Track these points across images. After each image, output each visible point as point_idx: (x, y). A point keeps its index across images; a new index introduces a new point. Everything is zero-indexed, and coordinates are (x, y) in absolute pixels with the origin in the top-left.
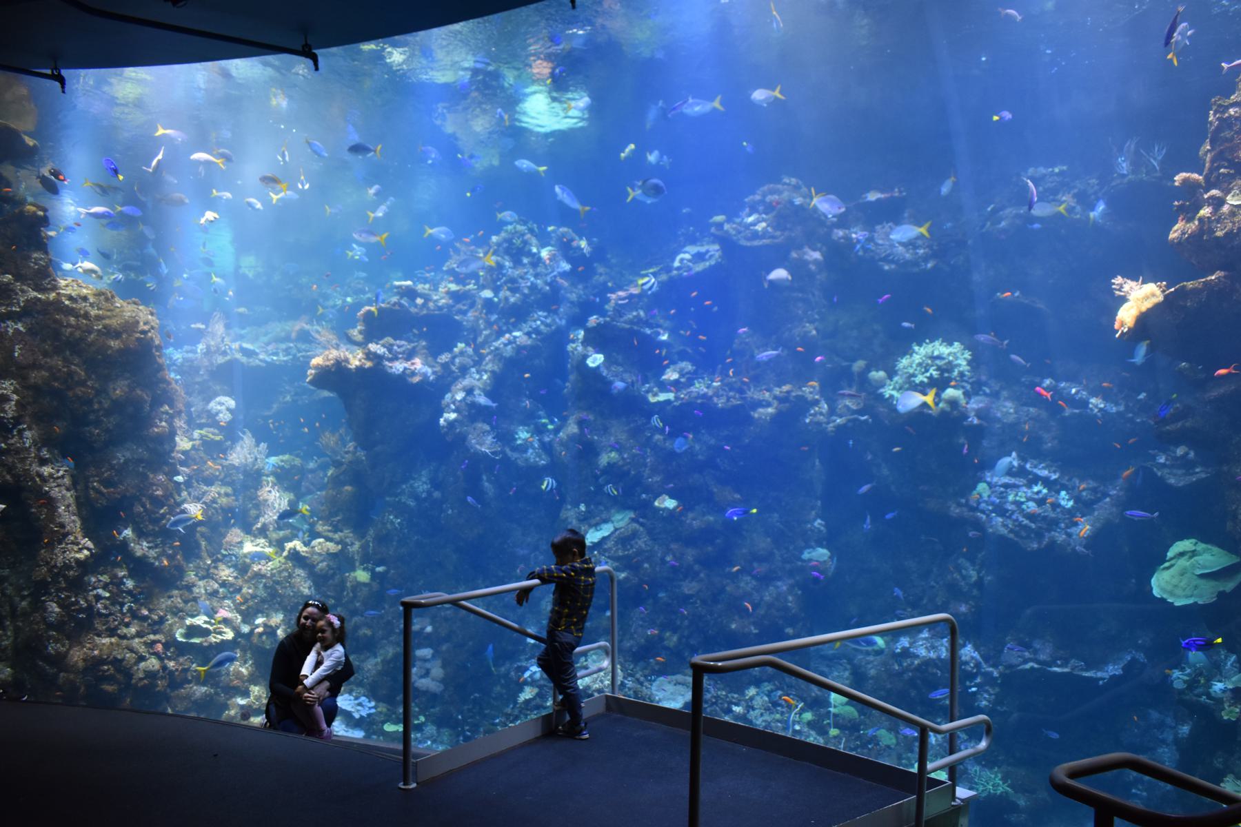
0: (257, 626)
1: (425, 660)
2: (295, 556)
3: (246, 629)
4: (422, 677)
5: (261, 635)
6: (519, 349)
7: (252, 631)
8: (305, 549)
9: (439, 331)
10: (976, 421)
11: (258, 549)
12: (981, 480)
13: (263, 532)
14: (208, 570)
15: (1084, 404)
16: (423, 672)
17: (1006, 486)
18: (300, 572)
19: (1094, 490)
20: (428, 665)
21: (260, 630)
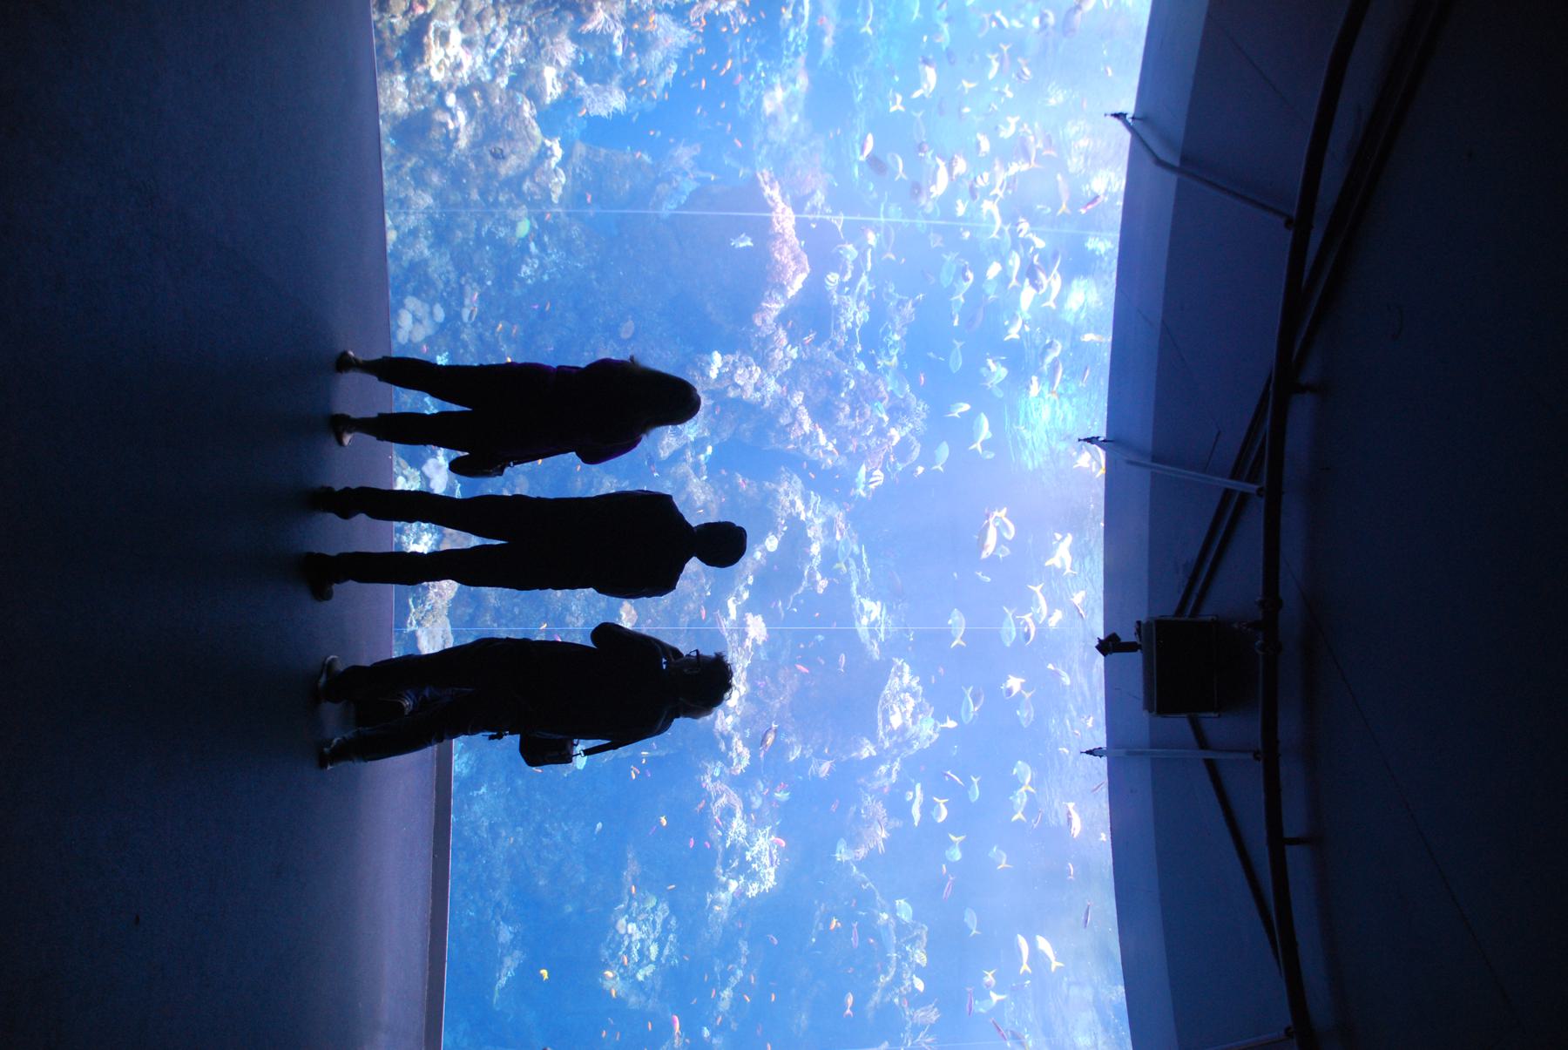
0: (454, 117)
1: (431, 314)
2: (544, 153)
3: (451, 100)
4: (414, 316)
5: (445, 125)
6: (784, 431)
7: (449, 110)
8: (553, 165)
9: (813, 315)
11: (549, 89)
12: (659, 898)
13: (570, 86)
14: (519, 23)
15: (725, 985)
16: (419, 314)
17: (654, 922)
18: (526, 164)
19: (653, 989)
20: (426, 322)
21: (451, 126)
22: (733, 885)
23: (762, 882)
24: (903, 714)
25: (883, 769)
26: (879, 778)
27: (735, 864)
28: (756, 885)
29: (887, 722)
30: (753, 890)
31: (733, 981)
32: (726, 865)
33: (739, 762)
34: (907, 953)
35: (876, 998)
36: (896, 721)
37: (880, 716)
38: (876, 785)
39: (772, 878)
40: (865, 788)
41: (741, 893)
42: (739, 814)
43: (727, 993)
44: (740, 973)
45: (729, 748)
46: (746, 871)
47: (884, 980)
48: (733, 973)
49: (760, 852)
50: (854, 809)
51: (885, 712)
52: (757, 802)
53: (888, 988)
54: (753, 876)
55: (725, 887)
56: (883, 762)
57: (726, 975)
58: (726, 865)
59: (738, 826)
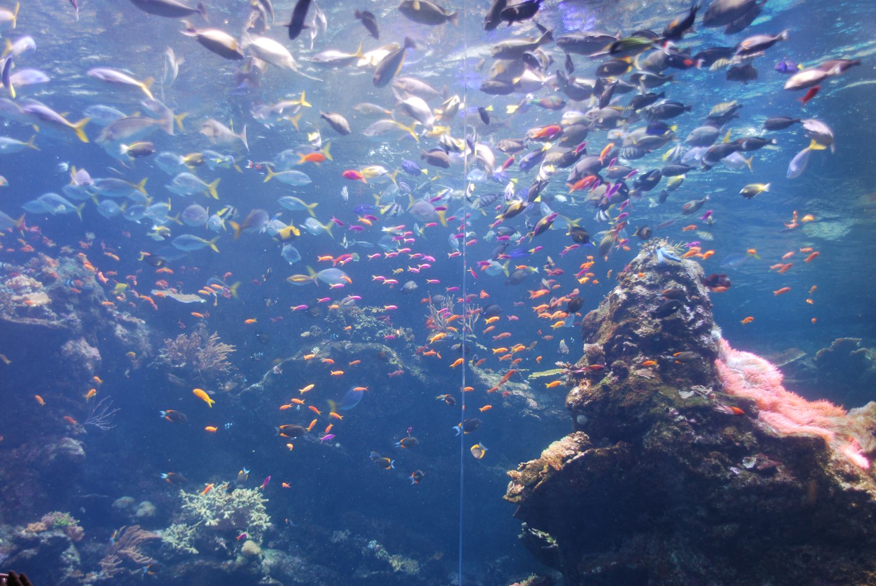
10: (271, 581)
22: (250, 546)
23: (252, 506)
24: (34, 289)
25: (120, 330)
26: (136, 340)
27: (222, 542)
28: (254, 515)
29: (38, 312)
30: (261, 519)
31: (382, 553)
32: (223, 555)
33: (64, 528)
34: (364, 329)
35: (416, 371)
36: (39, 299)
37: (28, 321)
38: (146, 345)
39: (249, 493)
40: (149, 359)
41: (268, 539)
42: (159, 534)
43: (396, 563)
44: (373, 544)
45: (33, 543)
46: (233, 529)
47: (395, 359)
48: (373, 551)
49: (210, 507)
50: (171, 377)
51: (24, 311)
52: (147, 508)
53: (406, 356)
54: (241, 516)
55: (252, 558)
56: (111, 330)
57: (372, 560)
58: (223, 555)
59: (170, 536)
